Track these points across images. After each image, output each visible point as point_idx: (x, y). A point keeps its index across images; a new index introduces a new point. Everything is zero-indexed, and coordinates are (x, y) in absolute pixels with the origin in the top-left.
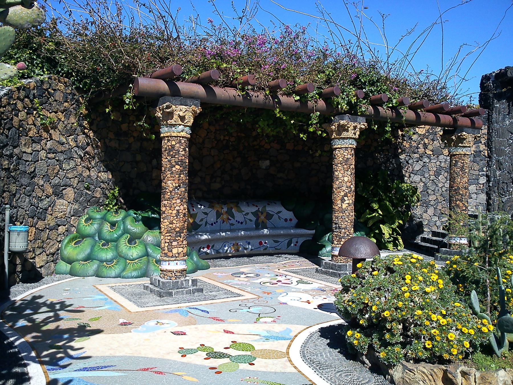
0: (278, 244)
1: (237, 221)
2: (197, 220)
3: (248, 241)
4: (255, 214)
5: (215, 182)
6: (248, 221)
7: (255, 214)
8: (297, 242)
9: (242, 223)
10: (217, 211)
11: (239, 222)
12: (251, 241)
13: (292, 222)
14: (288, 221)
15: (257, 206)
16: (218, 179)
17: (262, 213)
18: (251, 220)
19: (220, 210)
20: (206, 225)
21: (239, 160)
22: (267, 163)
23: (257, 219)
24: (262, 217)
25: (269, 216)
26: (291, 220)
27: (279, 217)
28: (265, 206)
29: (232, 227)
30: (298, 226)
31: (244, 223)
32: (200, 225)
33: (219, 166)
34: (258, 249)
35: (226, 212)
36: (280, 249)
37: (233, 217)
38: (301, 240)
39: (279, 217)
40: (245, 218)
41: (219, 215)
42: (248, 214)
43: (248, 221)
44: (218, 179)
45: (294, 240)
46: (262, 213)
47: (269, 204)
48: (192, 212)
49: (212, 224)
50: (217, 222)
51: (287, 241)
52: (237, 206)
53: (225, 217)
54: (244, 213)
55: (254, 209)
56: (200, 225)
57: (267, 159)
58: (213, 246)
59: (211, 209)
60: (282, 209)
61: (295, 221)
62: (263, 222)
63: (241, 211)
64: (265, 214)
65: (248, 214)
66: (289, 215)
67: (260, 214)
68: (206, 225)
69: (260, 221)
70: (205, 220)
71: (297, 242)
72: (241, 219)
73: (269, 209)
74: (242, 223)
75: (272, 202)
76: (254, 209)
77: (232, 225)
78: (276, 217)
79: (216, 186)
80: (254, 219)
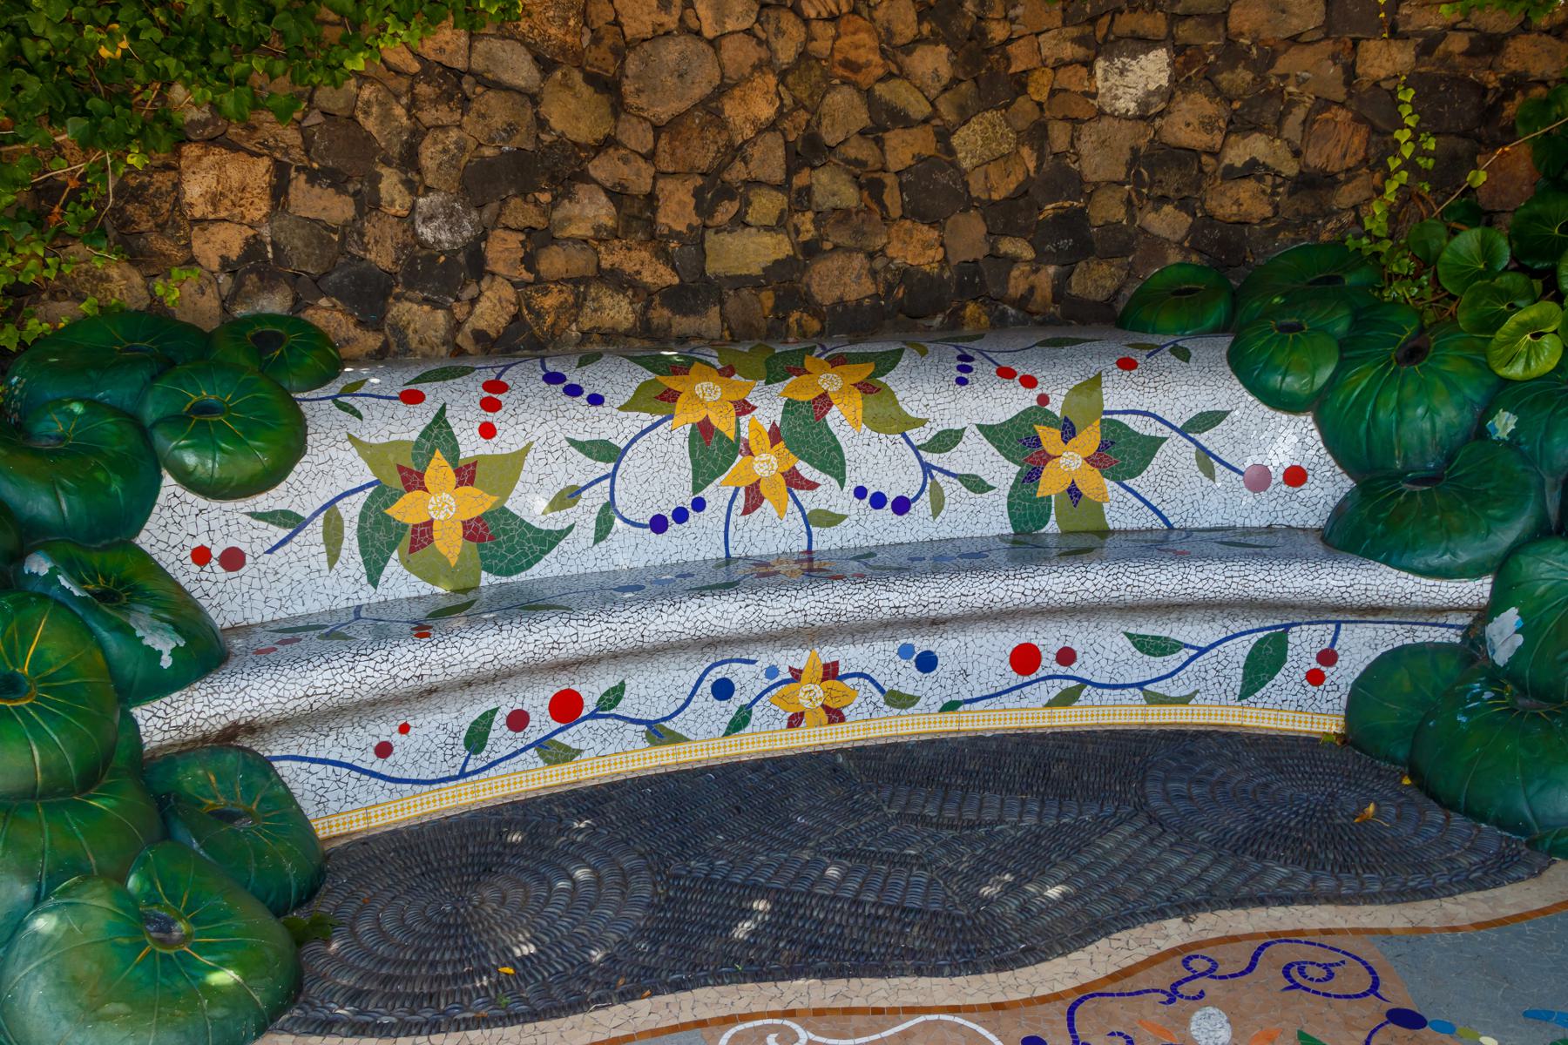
0: (1173, 661)
1: (860, 492)
2: (531, 504)
3: (921, 644)
4: (1018, 440)
5: (739, 221)
6: (951, 488)
7: (1018, 440)
8: (1328, 657)
9: (902, 506)
10: (704, 430)
11: (878, 501)
12: (944, 646)
13: (1305, 492)
14: (1279, 487)
15: (1029, 382)
16: (766, 205)
17: (1069, 431)
18: (976, 484)
19: (724, 423)
20: (603, 529)
21: (933, 62)
22: (1151, 70)
23: (1031, 476)
24: (1070, 462)
25: (1123, 453)
26: (1295, 476)
27: (1206, 459)
28: (1095, 383)
29: (827, 540)
30: (1346, 535)
31: (922, 507)
32: (549, 540)
33: (766, 111)
34: (1009, 701)
35: (775, 435)
36: (1184, 700)
37: (833, 462)
38: (1361, 647)
39: (1206, 459)
40: (927, 468)
41: (711, 451)
42: (947, 440)
43: (951, 488)
44: (766, 205)
45: (1305, 643)
46: (1069, 431)
47: (1127, 364)
48: (471, 445)
49: (658, 524)
50: (699, 505)
51: (1240, 649)
52: (868, 388)
53: (766, 464)
54: (919, 436)
55: (1004, 402)
56: (549, 540)
57: (1146, 43)
58: (614, 696)
59: (646, 419)
60: (1225, 392)
61: (1329, 486)
62: (1074, 492)
63: (895, 422)
64: (1090, 439)
65: (947, 440)
66: (1290, 440)
67: (1050, 437)
68: (603, 529)
69: (1051, 484)
70: (594, 499)
71: (1328, 657)
72: (900, 477)
73: (1119, 395)
74: (902, 506)
75: (1155, 350)
76: (1004, 402)
77: (816, 519)
78: (1176, 454)
79: (749, 251)
80: (1003, 473)
